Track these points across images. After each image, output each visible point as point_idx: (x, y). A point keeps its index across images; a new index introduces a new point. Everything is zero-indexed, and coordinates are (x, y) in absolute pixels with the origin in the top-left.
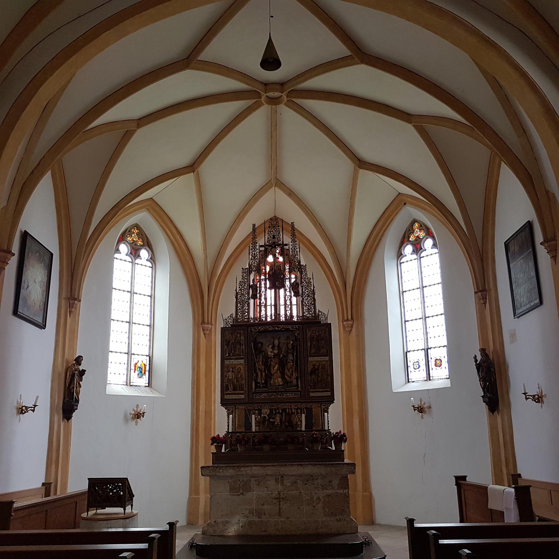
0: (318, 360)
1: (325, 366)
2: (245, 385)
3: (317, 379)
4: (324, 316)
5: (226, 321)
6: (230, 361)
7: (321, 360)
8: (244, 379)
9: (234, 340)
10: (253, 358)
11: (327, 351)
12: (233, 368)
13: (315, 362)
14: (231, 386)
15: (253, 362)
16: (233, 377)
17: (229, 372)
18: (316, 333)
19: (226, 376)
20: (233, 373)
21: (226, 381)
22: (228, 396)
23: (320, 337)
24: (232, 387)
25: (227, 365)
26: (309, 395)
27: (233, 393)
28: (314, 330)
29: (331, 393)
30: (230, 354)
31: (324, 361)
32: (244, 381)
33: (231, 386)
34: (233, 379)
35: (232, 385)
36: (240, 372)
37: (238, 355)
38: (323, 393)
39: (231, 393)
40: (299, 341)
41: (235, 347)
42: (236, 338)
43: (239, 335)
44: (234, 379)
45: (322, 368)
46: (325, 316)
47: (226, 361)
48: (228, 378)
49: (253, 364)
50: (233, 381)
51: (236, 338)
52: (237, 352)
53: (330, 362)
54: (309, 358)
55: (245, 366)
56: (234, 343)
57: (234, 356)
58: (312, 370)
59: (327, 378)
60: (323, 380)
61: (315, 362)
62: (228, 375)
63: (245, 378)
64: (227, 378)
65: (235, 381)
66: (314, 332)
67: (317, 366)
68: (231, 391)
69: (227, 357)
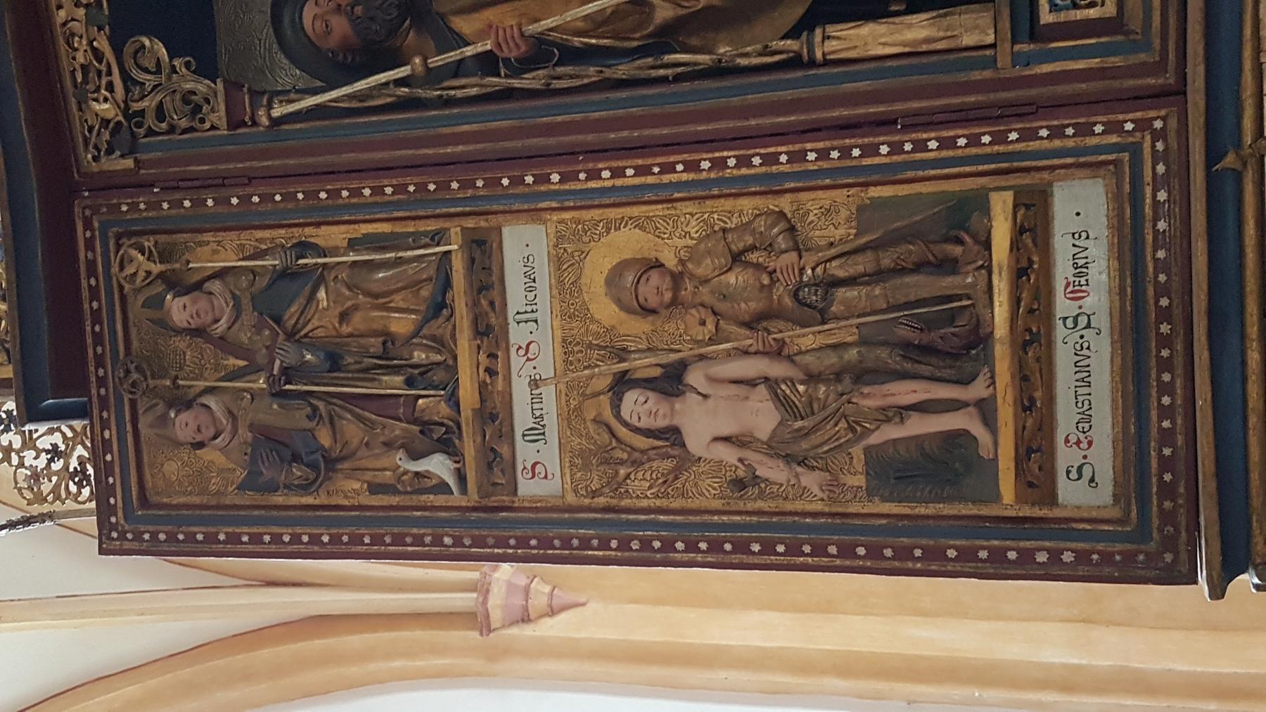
2: (888, 175)
5: (46, 487)
6: (522, 419)
8: (785, 203)
9: (252, 369)
10: (472, 86)
12: (622, 383)
14: (903, 412)
15: (528, 81)
16: (751, 383)
17: (672, 435)
19: (739, 485)
20: (695, 377)
21: (811, 480)
22: (1065, 457)
24: (906, 392)
25: (577, 459)
27: (1023, 378)
30: (426, 426)
32: (814, 202)
33: (903, 412)
34: (777, 369)
35: (872, 398)
36: (677, 279)
37: (439, 306)
39: (1026, 405)
41: (334, 362)
42: (224, 344)
43: (179, 310)
44: (778, 352)
47: (528, 488)
48: (777, 448)
49: (568, 75)
50: (812, 378)
51: (224, 344)
52: (401, 324)
55: (588, 200)
56: (288, 373)
57: (453, 369)
62: (728, 454)
63: (771, 186)
64: (773, 471)
65: (808, 339)
68: (986, 409)
69: (461, 477)
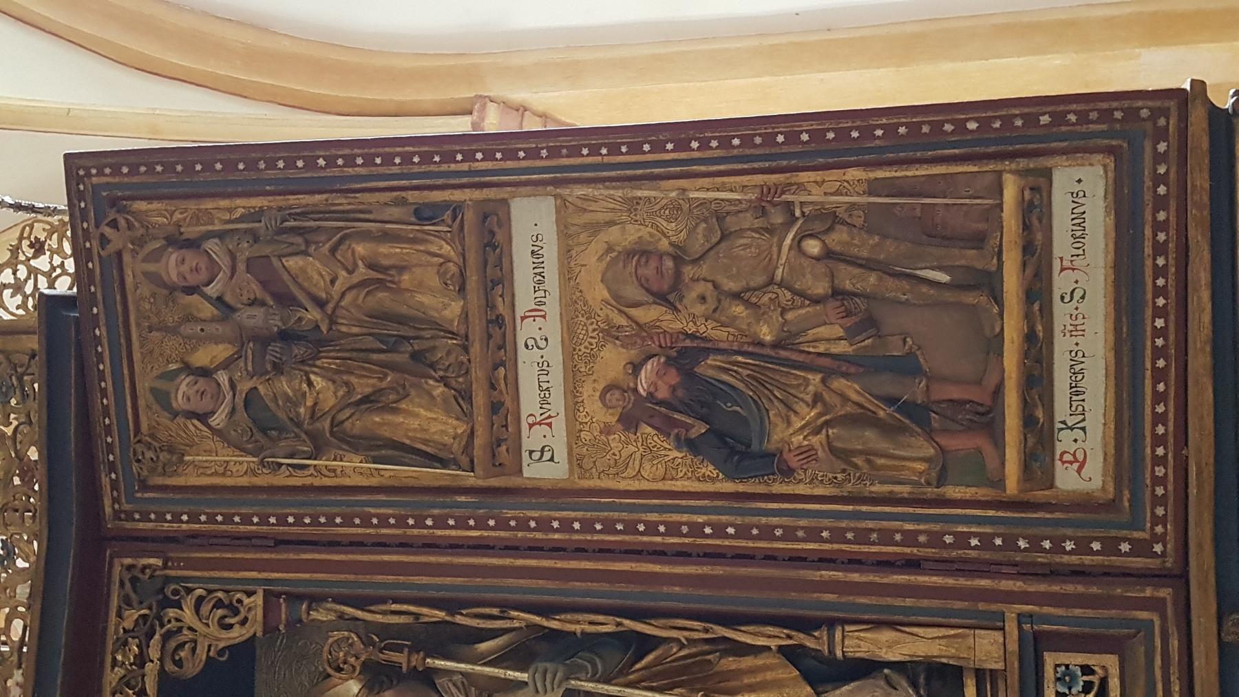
0: (555, 354)
1: (641, 253)
3: (833, 366)
4: (42, 263)
7: (553, 308)
11: (425, 214)
13: (590, 392)
18: (205, 373)
23: (253, 318)
26: (1083, 504)
28: (163, 399)
29: (1078, 148)
31: (568, 274)
38: (1061, 283)
40: (315, 600)
45: (666, 298)
46: (38, 247)
53: (595, 176)
54: (534, 471)
58: (692, 446)
59: (829, 219)
60: (849, 278)
61: (590, 392)
66: (184, 391)
67: (636, 368)
